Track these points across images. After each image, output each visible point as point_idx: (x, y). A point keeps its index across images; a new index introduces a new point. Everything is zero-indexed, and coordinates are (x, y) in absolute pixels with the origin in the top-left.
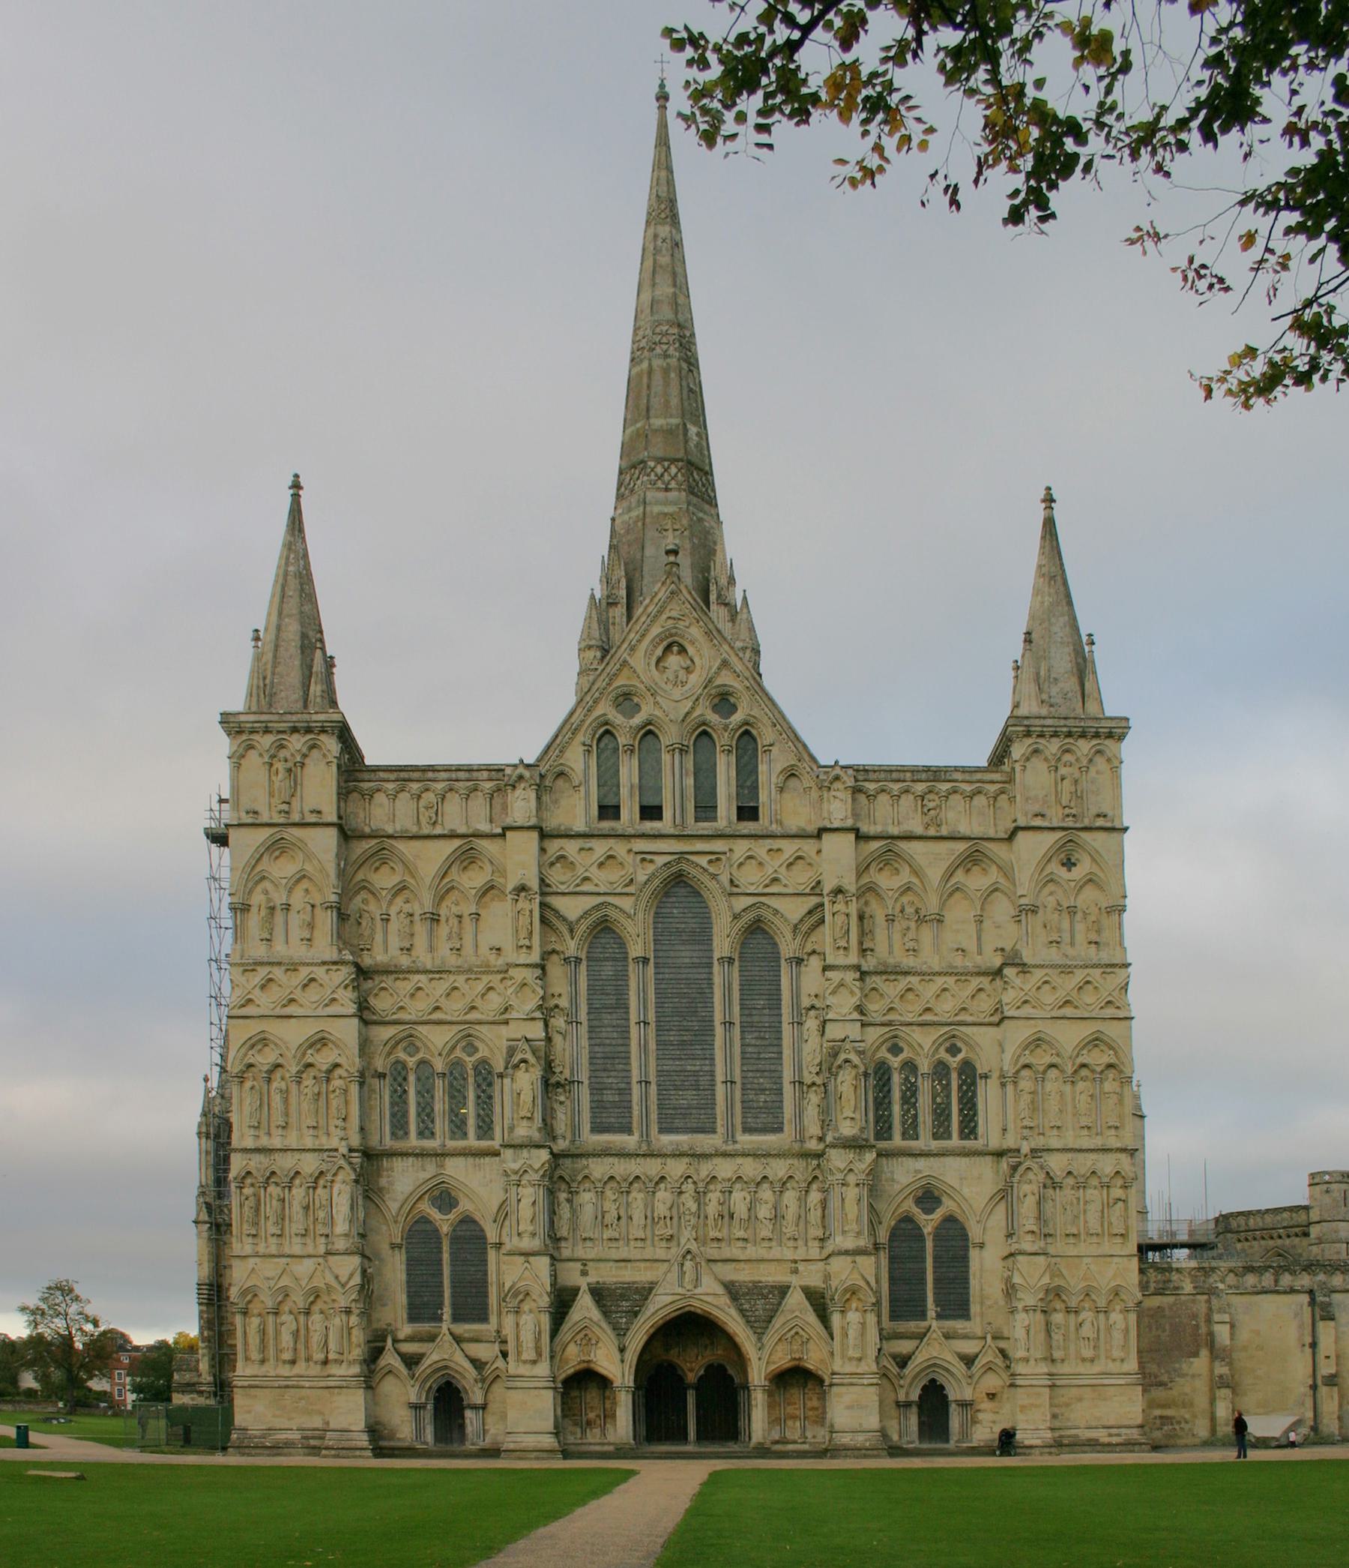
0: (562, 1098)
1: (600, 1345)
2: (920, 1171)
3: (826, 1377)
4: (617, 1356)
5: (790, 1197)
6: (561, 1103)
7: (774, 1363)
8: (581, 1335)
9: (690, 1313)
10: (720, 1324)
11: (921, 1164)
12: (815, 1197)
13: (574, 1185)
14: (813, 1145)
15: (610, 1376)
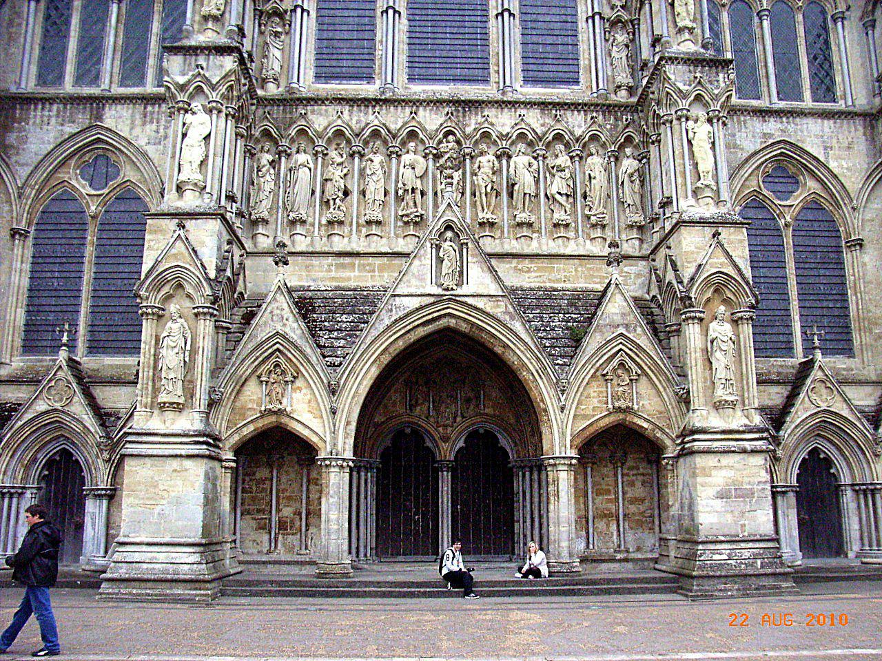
0: (279, 29)
1: (299, 383)
2: (771, 135)
3: (668, 442)
4: (324, 401)
5: (596, 163)
6: (277, 35)
7: (585, 417)
8: (269, 365)
9: (448, 329)
10: (499, 350)
11: (773, 127)
12: (629, 164)
13: (284, 142)
14: (622, 97)
15: (315, 439)
